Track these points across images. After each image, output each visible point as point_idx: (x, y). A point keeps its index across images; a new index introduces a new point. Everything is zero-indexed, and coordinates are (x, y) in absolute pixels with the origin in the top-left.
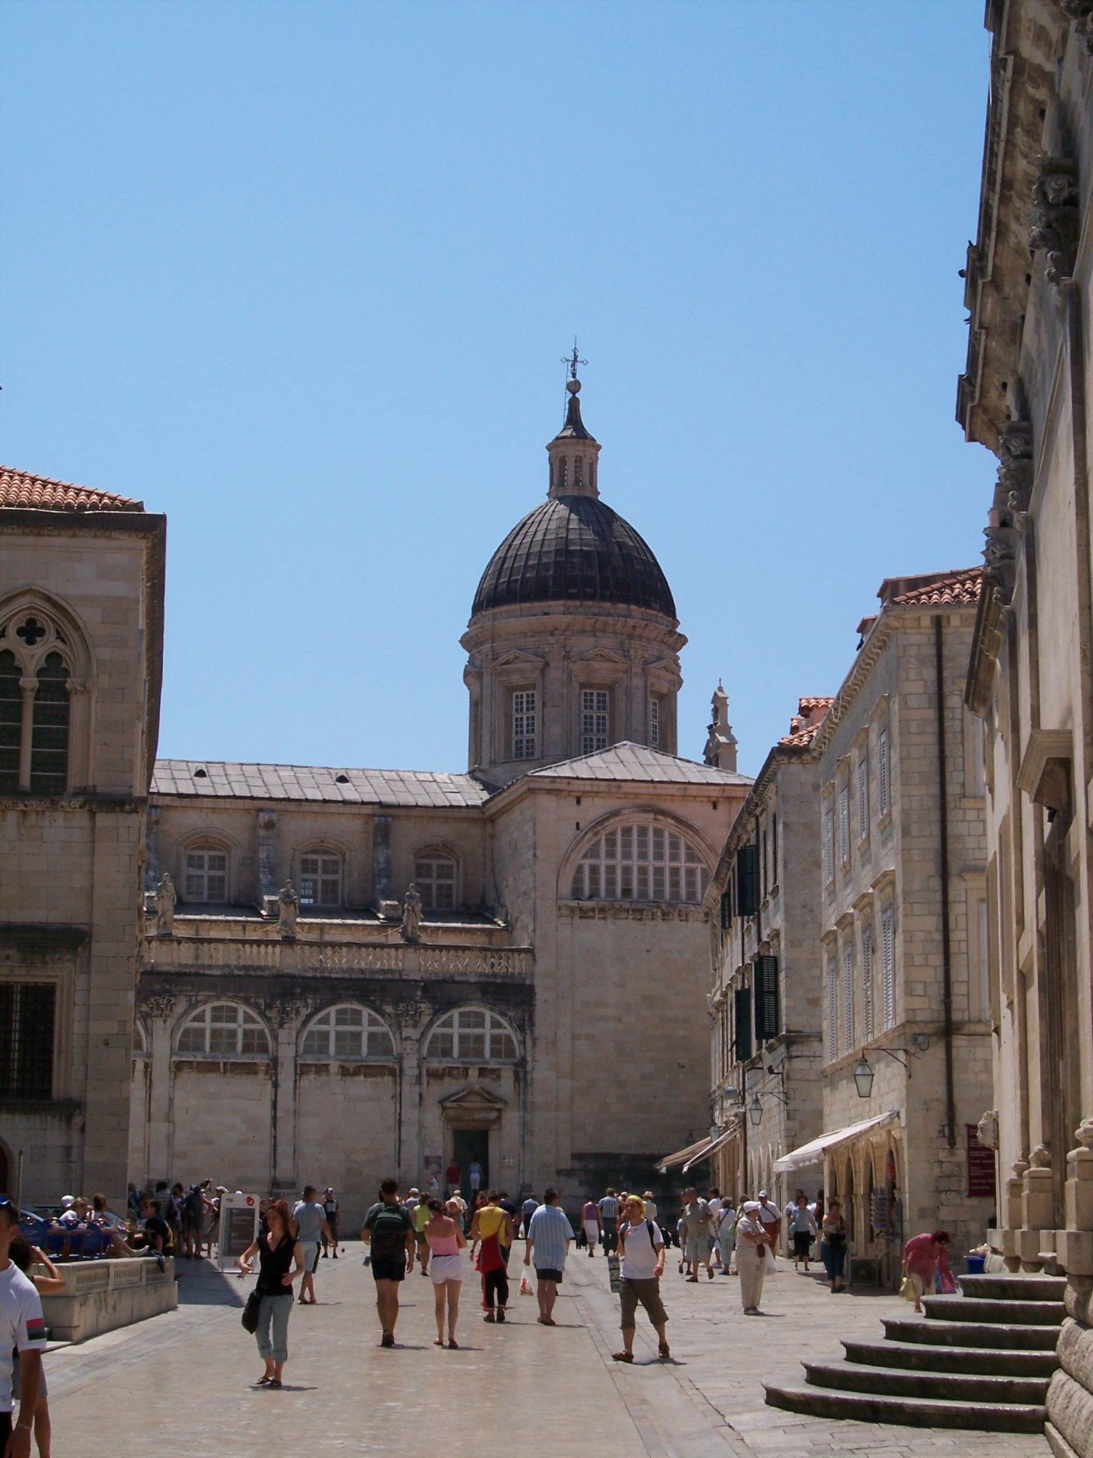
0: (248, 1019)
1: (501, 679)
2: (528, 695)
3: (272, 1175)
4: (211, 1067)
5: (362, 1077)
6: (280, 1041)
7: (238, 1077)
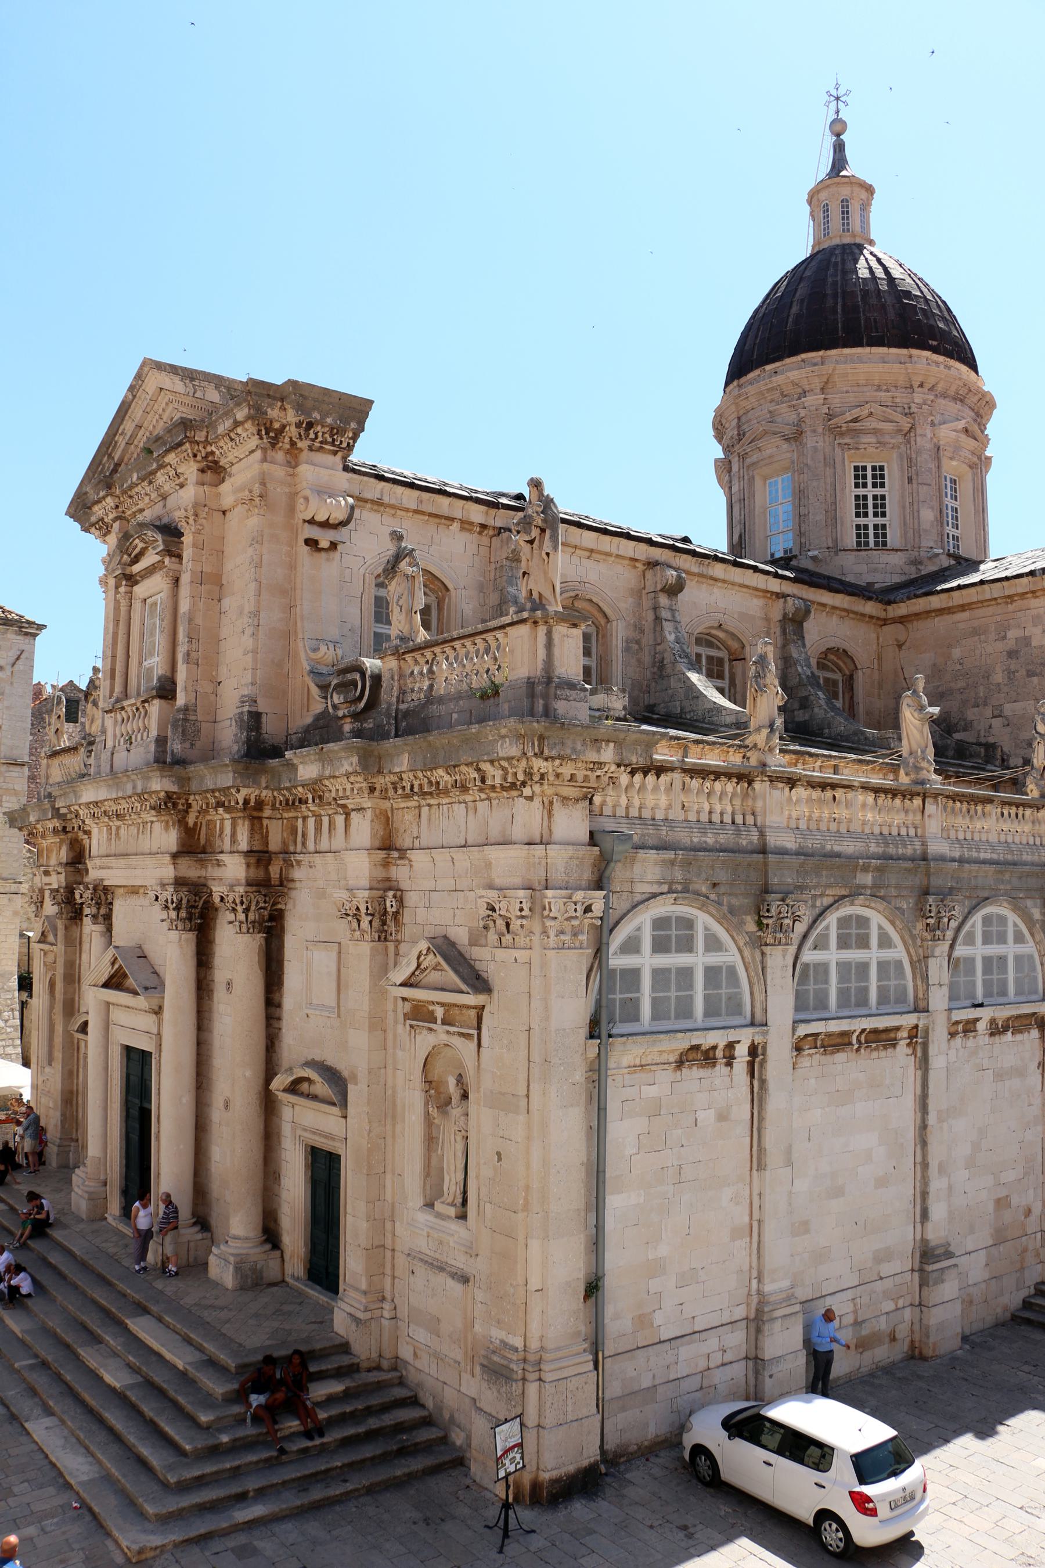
0: (885, 942)
3: (918, 1237)
4: (840, 1042)
6: (930, 982)
7: (875, 1054)
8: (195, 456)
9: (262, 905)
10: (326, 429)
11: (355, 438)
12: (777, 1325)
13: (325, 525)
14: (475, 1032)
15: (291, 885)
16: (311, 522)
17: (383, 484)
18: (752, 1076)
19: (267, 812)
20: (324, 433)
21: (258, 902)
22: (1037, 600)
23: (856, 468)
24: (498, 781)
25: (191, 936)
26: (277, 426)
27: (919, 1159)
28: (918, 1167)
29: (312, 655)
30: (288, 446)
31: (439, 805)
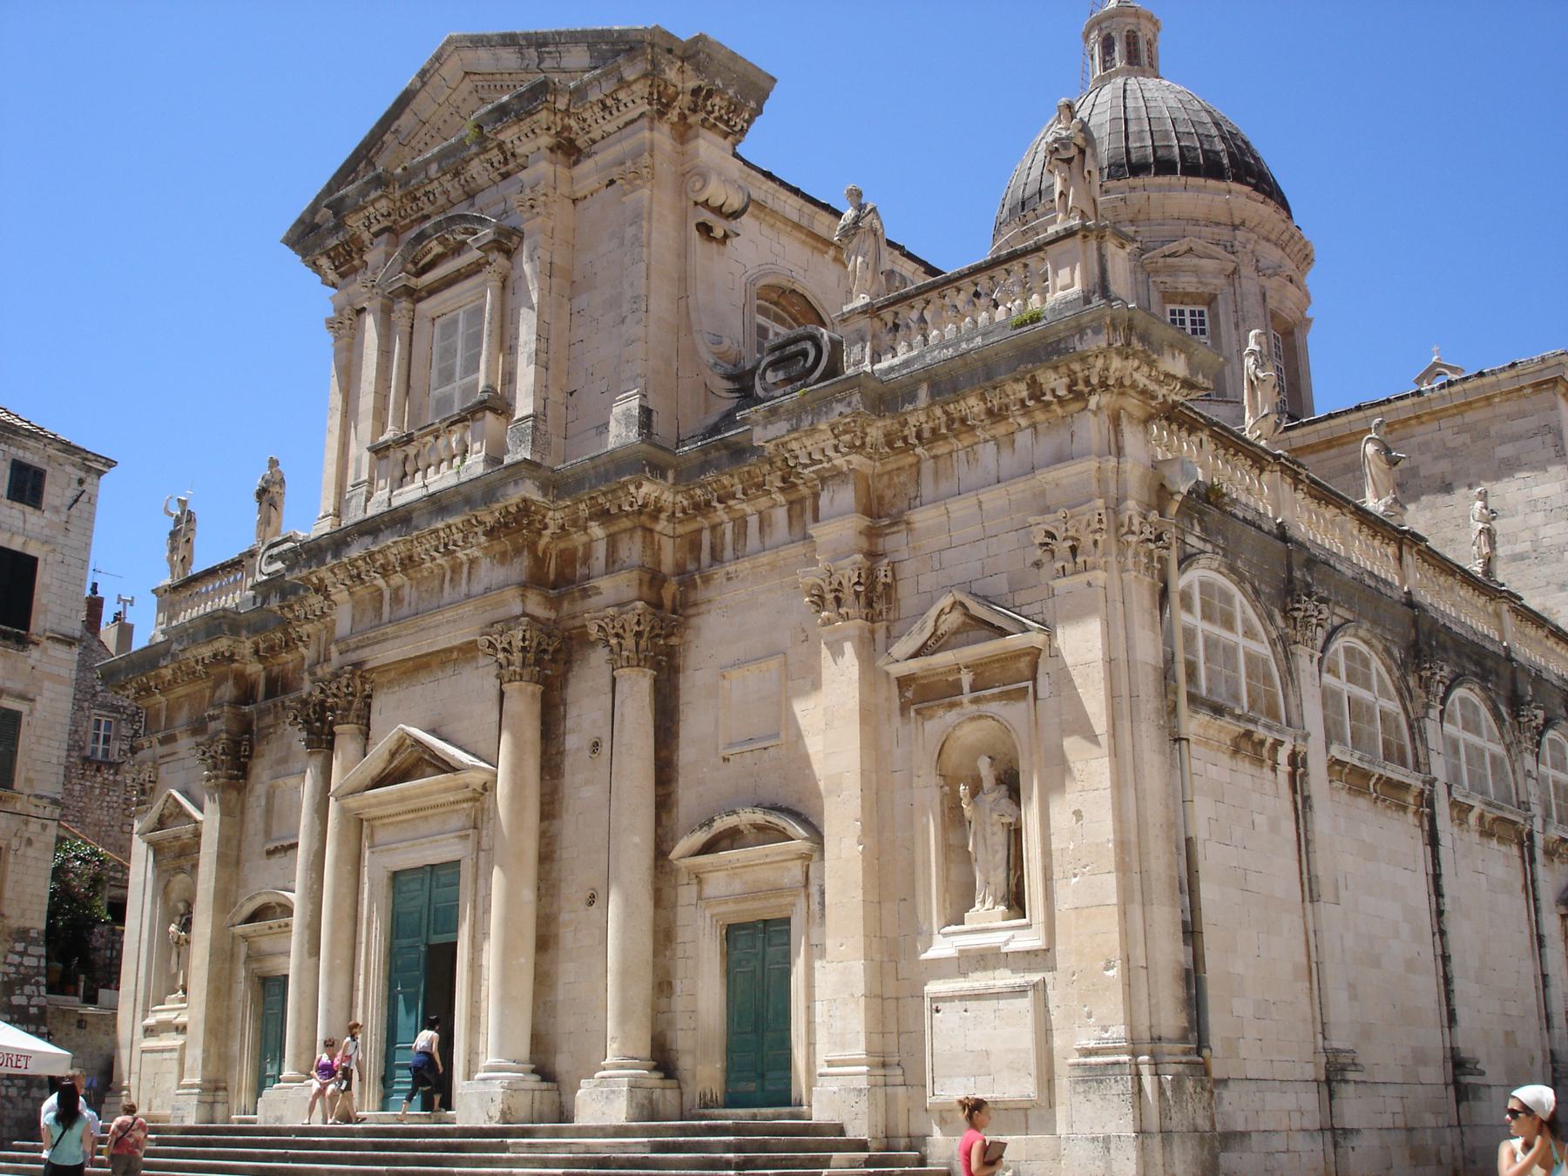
1: (1159, 280)
2: (1192, 313)
3: (1448, 1045)
5: (1494, 842)
7: (1389, 812)
8: (549, 129)
9: (657, 631)
10: (725, 103)
11: (749, 122)
12: (1351, 1088)
13: (718, 211)
14: (1030, 684)
15: (691, 611)
16: (706, 204)
17: (770, 183)
18: (1295, 791)
19: (662, 525)
20: (721, 108)
21: (653, 628)
22: (1423, 427)
23: (1173, 313)
24: (1062, 392)
25: (539, 688)
26: (671, 90)
27: (1439, 951)
28: (1439, 959)
29: (715, 348)
30: (675, 119)
31: (950, 453)
